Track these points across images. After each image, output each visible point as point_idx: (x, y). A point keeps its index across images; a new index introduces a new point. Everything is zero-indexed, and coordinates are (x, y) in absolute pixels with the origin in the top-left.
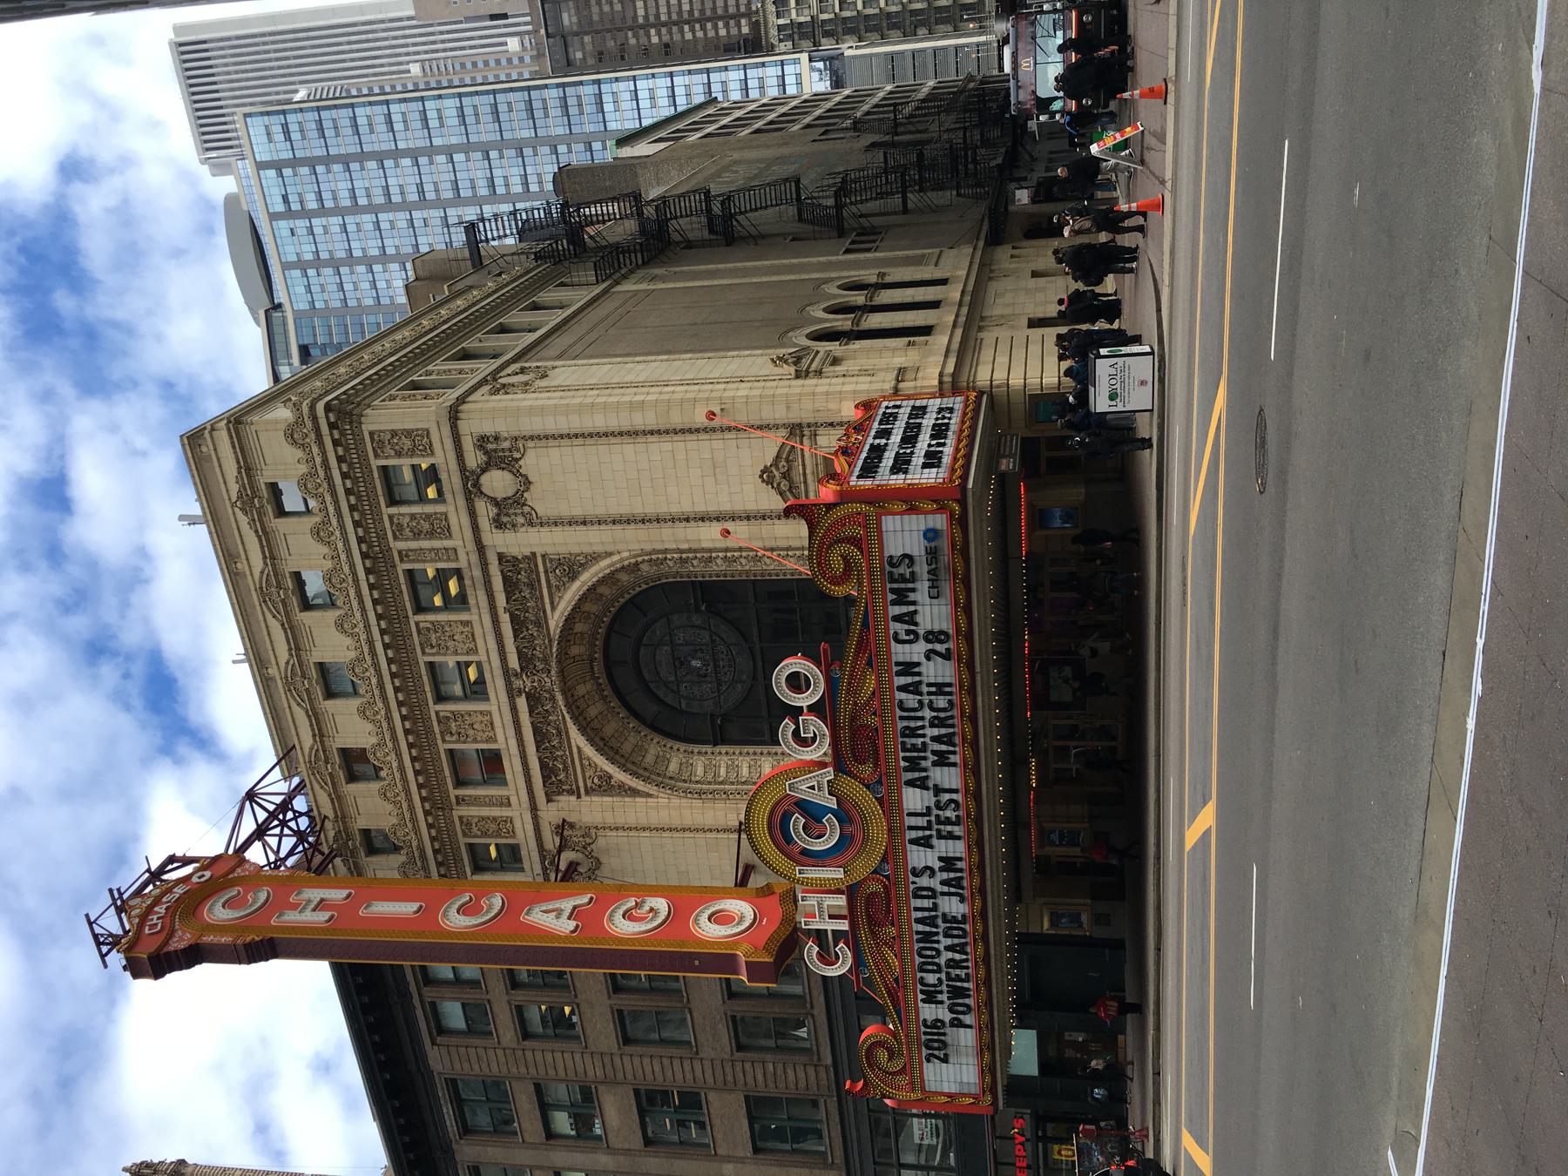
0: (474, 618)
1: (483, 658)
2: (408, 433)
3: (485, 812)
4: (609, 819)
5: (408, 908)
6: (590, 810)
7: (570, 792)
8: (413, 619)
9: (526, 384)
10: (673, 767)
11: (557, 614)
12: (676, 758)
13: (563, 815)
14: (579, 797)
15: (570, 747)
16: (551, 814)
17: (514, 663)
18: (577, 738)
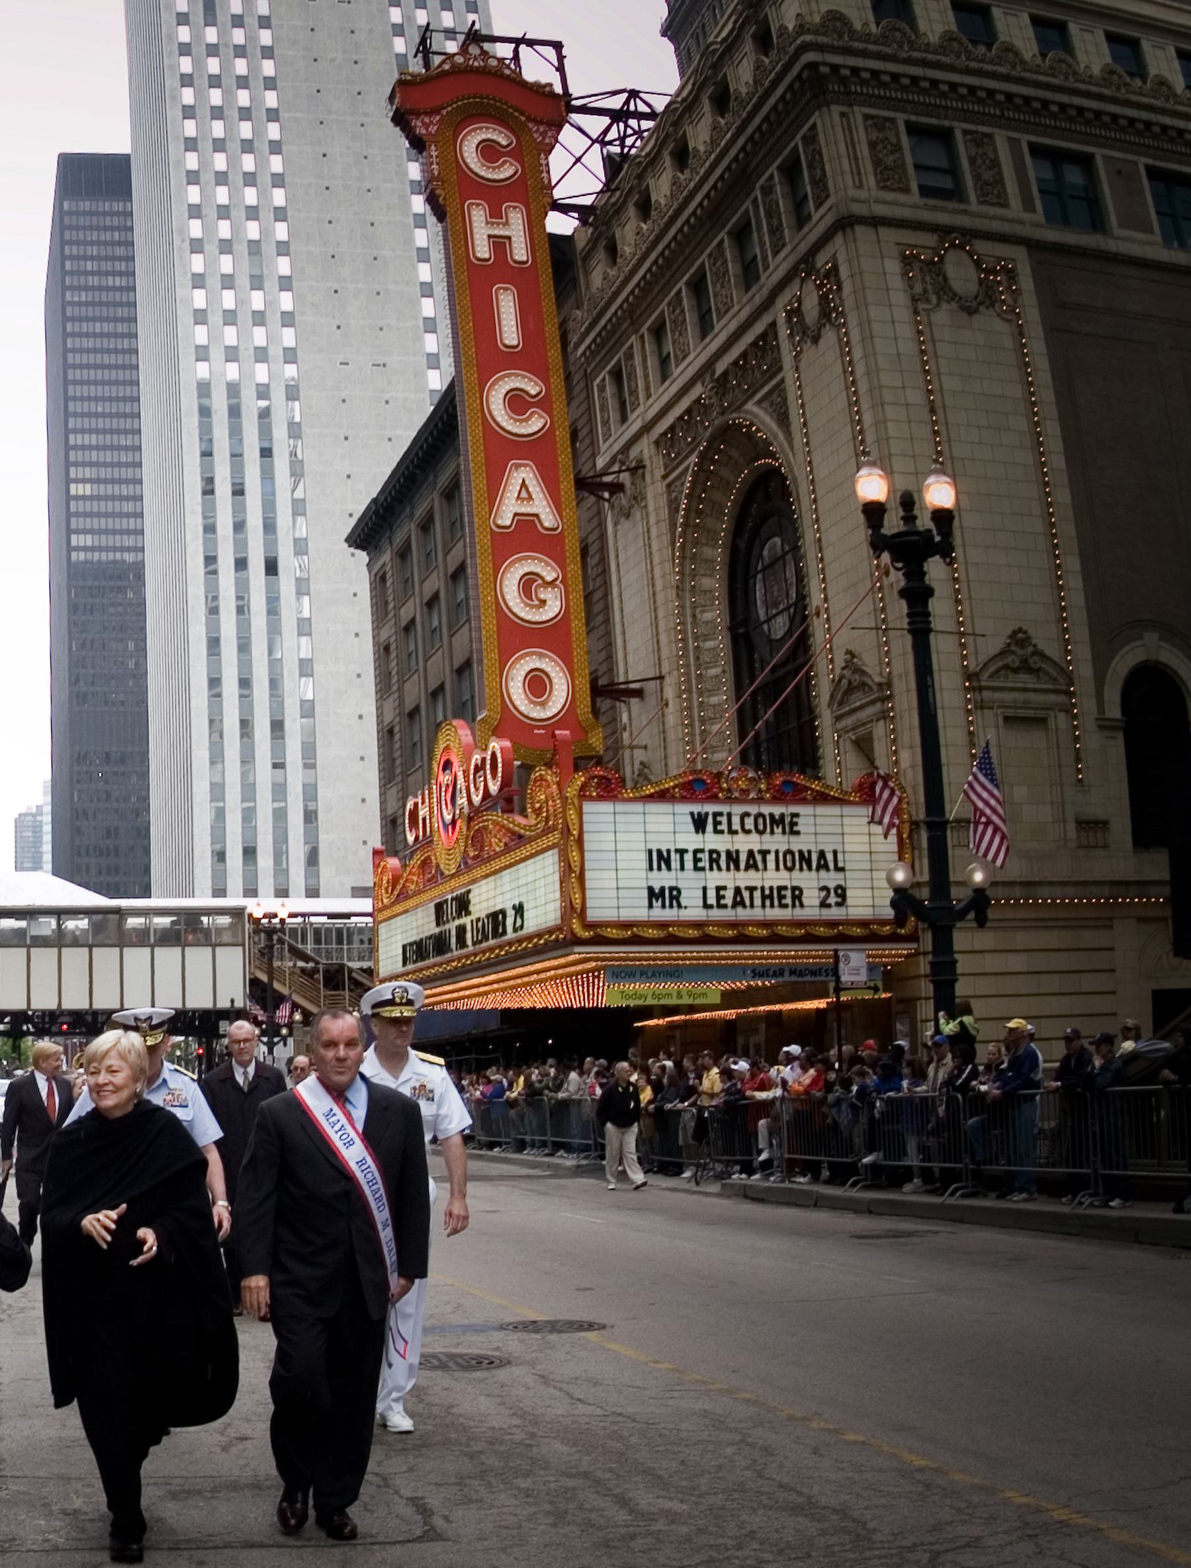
0: (736, 308)
1: (716, 330)
2: (824, 174)
3: (639, 372)
4: (652, 519)
5: (510, 333)
6: (655, 492)
7: (666, 467)
8: (723, 234)
9: (944, 291)
10: (707, 582)
11: (755, 409)
12: (714, 583)
13: (647, 463)
14: (664, 477)
15: (686, 457)
16: (645, 449)
17: (720, 367)
18: (694, 459)
